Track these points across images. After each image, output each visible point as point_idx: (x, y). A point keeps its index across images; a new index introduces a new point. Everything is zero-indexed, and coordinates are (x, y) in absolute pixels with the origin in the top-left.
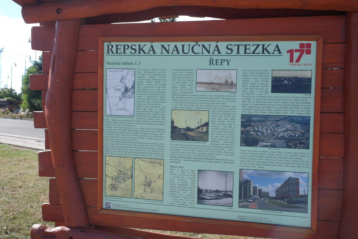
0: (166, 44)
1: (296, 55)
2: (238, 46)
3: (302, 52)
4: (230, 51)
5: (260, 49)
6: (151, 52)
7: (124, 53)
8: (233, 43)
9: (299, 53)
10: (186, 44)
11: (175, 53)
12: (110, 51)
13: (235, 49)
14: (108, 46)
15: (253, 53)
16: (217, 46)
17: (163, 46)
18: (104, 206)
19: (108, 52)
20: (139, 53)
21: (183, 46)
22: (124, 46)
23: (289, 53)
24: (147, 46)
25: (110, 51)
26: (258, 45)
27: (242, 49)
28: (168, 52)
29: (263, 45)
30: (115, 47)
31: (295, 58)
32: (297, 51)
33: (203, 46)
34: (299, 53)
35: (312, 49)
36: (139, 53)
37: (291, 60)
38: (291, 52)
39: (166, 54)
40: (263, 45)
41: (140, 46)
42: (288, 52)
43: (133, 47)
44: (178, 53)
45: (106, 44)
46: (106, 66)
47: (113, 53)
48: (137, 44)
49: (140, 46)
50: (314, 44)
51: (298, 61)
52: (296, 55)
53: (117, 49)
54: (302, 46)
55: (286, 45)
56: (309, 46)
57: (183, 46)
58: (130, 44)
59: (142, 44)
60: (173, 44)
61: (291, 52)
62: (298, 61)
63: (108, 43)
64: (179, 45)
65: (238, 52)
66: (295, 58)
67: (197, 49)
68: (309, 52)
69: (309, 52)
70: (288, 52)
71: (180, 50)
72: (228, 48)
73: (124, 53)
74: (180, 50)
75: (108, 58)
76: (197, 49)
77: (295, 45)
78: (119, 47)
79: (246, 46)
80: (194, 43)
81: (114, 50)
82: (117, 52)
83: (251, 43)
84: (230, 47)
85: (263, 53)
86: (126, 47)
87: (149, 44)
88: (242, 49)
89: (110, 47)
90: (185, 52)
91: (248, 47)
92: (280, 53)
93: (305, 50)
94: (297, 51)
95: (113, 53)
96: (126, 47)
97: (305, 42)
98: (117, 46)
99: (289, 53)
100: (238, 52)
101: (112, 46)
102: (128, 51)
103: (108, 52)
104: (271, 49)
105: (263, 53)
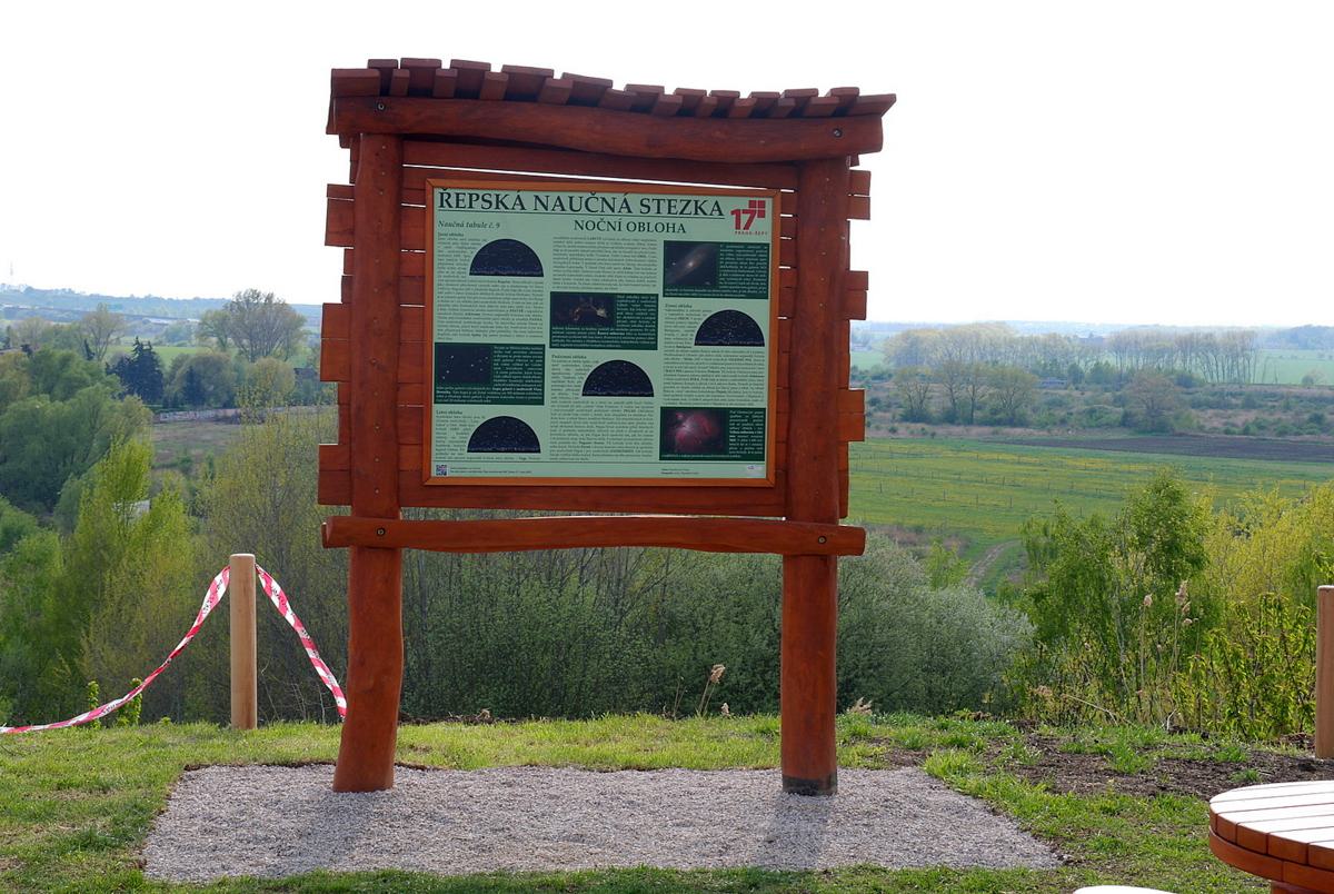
0: (542, 195)
2: (659, 200)
3: (753, 214)
4: (646, 210)
5: (691, 207)
6: (518, 208)
7: (471, 207)
8: (650, 197)
9: (749, 215)
10: (576, 195)
11: (558, 209)
12: (445, 203)
13: (654, 206)
14: (442, 194)
15: (681, 213)
16: (625, 200)
17: (537, 197)
18: (434, 473)
19: (442, 206)
20: (497, 208)
21: (571, 198)
22: (471, 195)
23: (734, 216)
24: (510, 198)
25: (445, 203)
26: (689, 201)
27: (664, 206)
28: (546, 208)
29: (696, 202)
30: (453, 197)
31: (743, 225)
32: (745, 212)
33: (604, 199)
34: (749, 215)
35: (766, 209)
36: (497, 208)
37: (738, 227)
38: (737, 213)
39: (543, 210)
40: (696, 202)
41: (498, 196)
42: (733, 213)
43: (486, 197)
44: (563, 210)
45: (437, 192)
46: (438, 229)
47: (450, 206)
48: (493, 193)
49: (498, 196)
50: (769, 202)
51: (747, 227)
52: (745, 218)
53: (458, 200)
54: (752, 204)
55: (730, 204)
56: (762, 204)
57: (571, 198)
58: (481, 193)
59: (502, 194)
60: (553, 196)
61: (737, 213)
62: (747, 227)
63: (442, 191)
64: (565, 197)
65: (659, 212)
66: (743, 225)
67: (595, 204)
68: (762, 215)
69: (762, 215)
70: (733, 213)
71: (566, 205)
72: (642, 205)
73: (471, 207)
74: (566, 205)
75: (440, 215)
76: (594, 204)
77: (743, 203)
78: (461, 197)
79: (670, 201)
80: (590, 195)
81: (453, 201)
82: (457, 206)
83: (679, 197)
84: (645, 202)
85: (696, 213)
86: (474, 197)
87: (513, 195)
88: (664, 206)
89: (445, 197)
90: (574, 208)
91: (673, 203)
92: (721, 214)
93: (756, 210)
94: (745, 212)
95: (450, 206)
96: (474, 197)
97: (757, 199)
98: (458, 194)
99: (734, 216)
100: (659, 212)
101: (449, 195)
102: (477, 205)
103: (442, 206)
104: (708, 207)
105: (696, 213)
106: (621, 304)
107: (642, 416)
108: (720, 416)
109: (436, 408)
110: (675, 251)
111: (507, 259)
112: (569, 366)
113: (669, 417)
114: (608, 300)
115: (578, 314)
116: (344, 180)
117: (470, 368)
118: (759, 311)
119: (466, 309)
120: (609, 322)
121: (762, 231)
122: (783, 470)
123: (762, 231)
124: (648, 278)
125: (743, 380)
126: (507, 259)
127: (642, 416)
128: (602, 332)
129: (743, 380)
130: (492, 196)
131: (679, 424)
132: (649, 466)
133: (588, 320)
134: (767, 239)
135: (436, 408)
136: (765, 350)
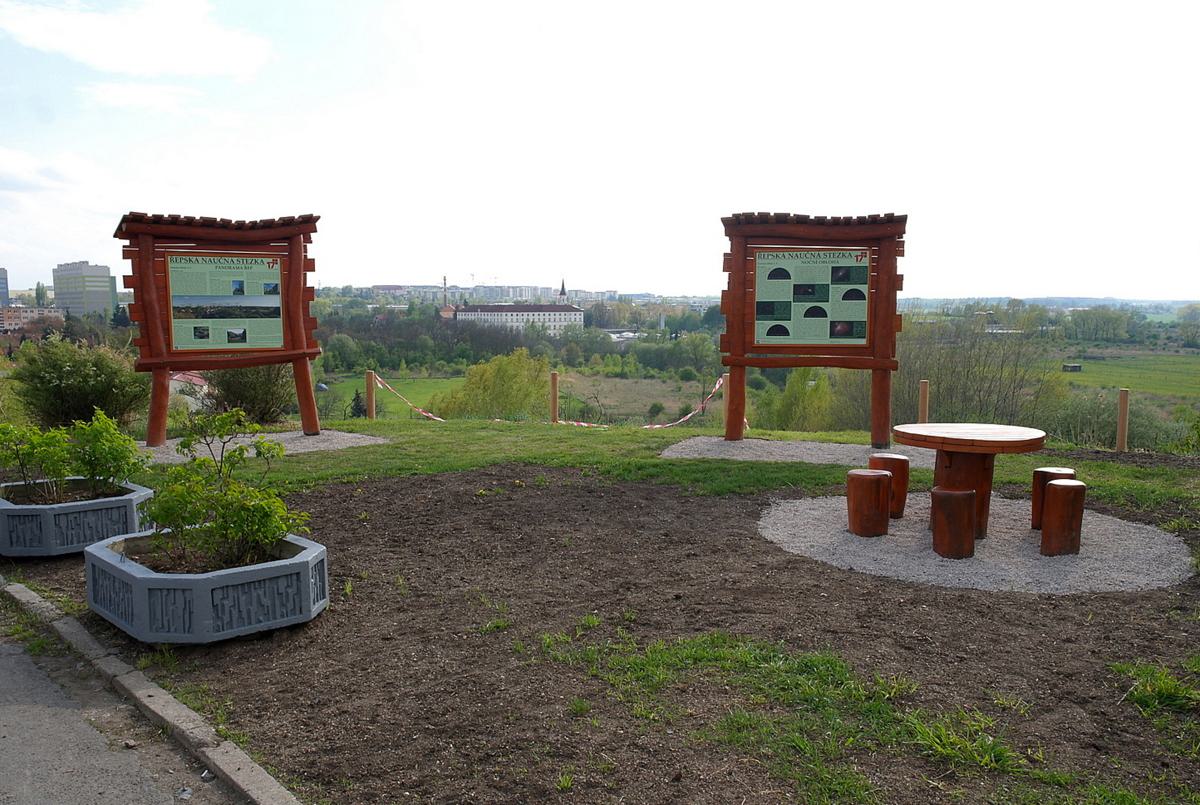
1: (859, 258)
38: (857, 256)
52: (859, 258)
61: (857, 256)
93: (864, 255)
106: (817, 287)
107: (823, 324)
108: (850, 324)
109: (756, 322)
110: (835, 270)
111: (780, 274)
112: (799, 308)
113: (833, 324)
114: (812, 286)
115: (802, 292)
116: (729, 251)
117: (767, 309)
118: (864, 289)
119: (766, 291)
120: (813, 293)
121: (866, 262)
122: (872, 341)
123: (866, 262)
124: (826, 278)
125: (859, 311)
126: (780, 274)
127: (823, 324)
128: (811, 296)
129: (859, 311)
130: (774, 254)
131: (836, 326)
132: (826, 340)
133: (806, 293)
134: (867, 265)
135: (756, 322)
136: (866, 302)
